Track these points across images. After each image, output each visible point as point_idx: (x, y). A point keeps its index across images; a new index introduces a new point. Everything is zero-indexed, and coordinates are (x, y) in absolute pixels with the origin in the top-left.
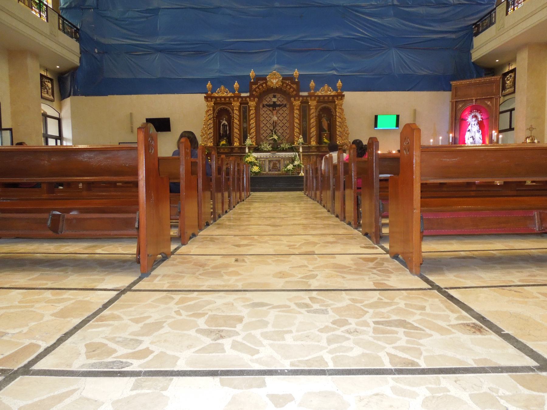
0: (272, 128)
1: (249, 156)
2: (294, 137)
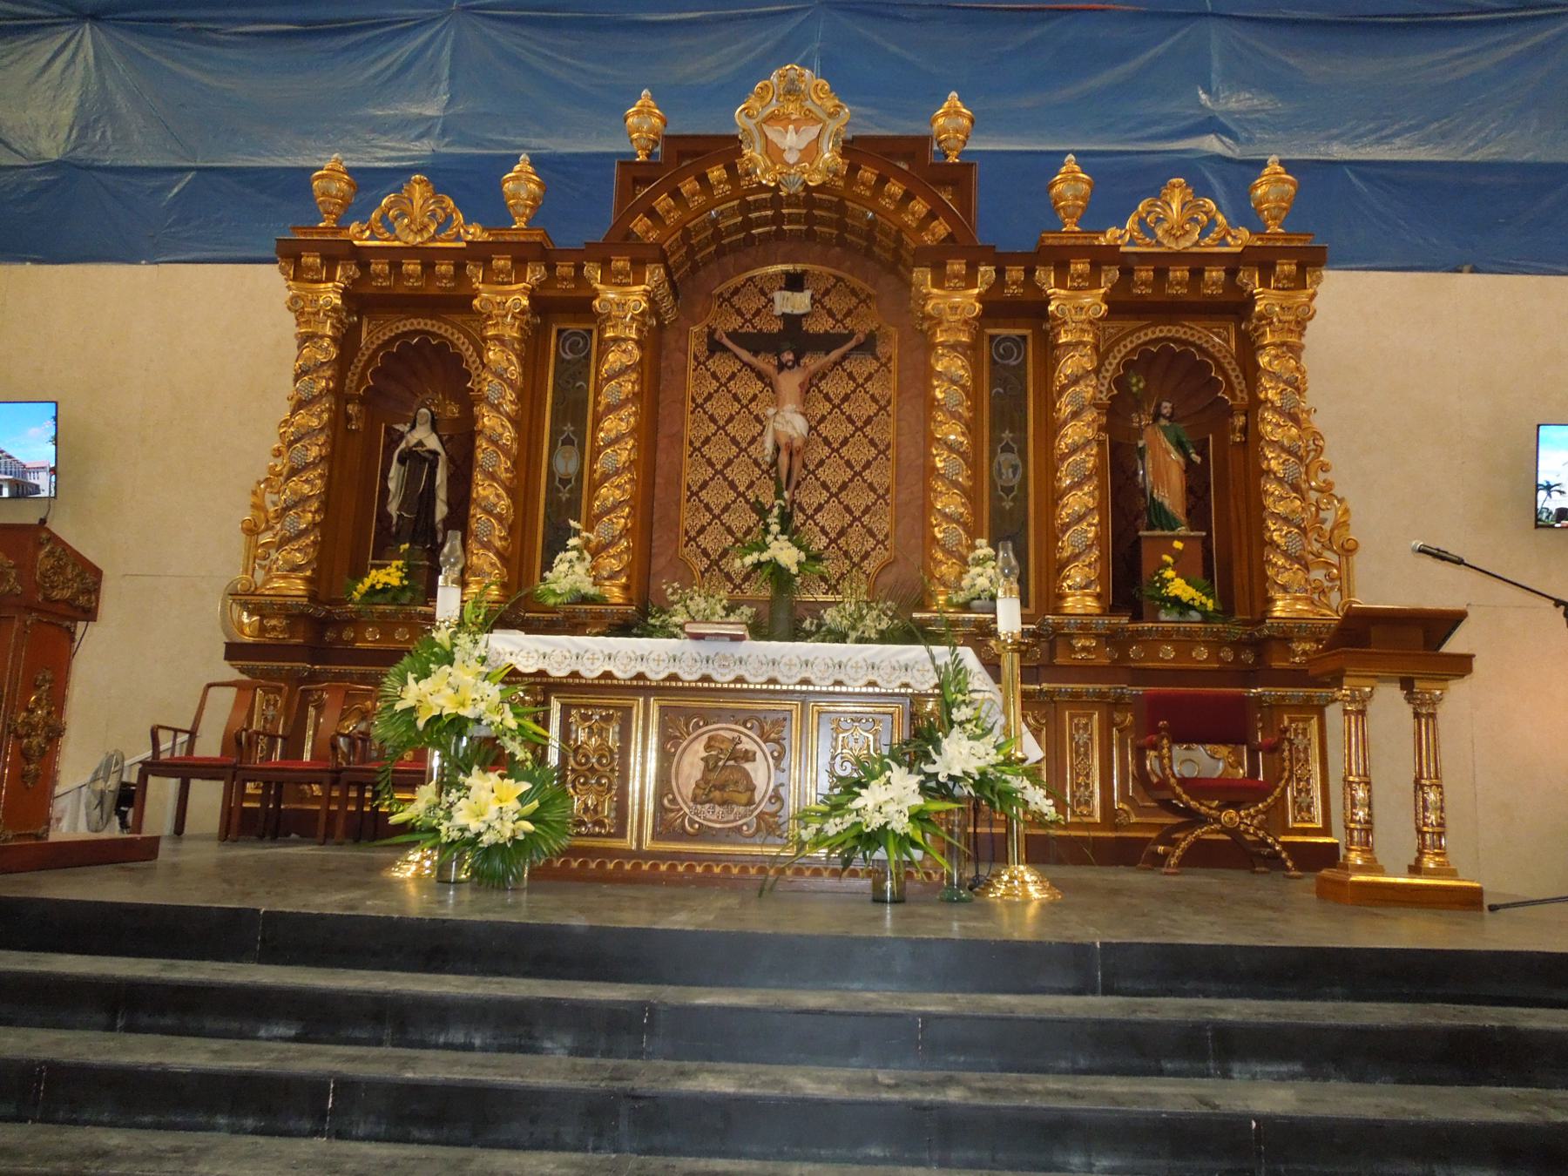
1: (448, 659)
2: (928, 563)
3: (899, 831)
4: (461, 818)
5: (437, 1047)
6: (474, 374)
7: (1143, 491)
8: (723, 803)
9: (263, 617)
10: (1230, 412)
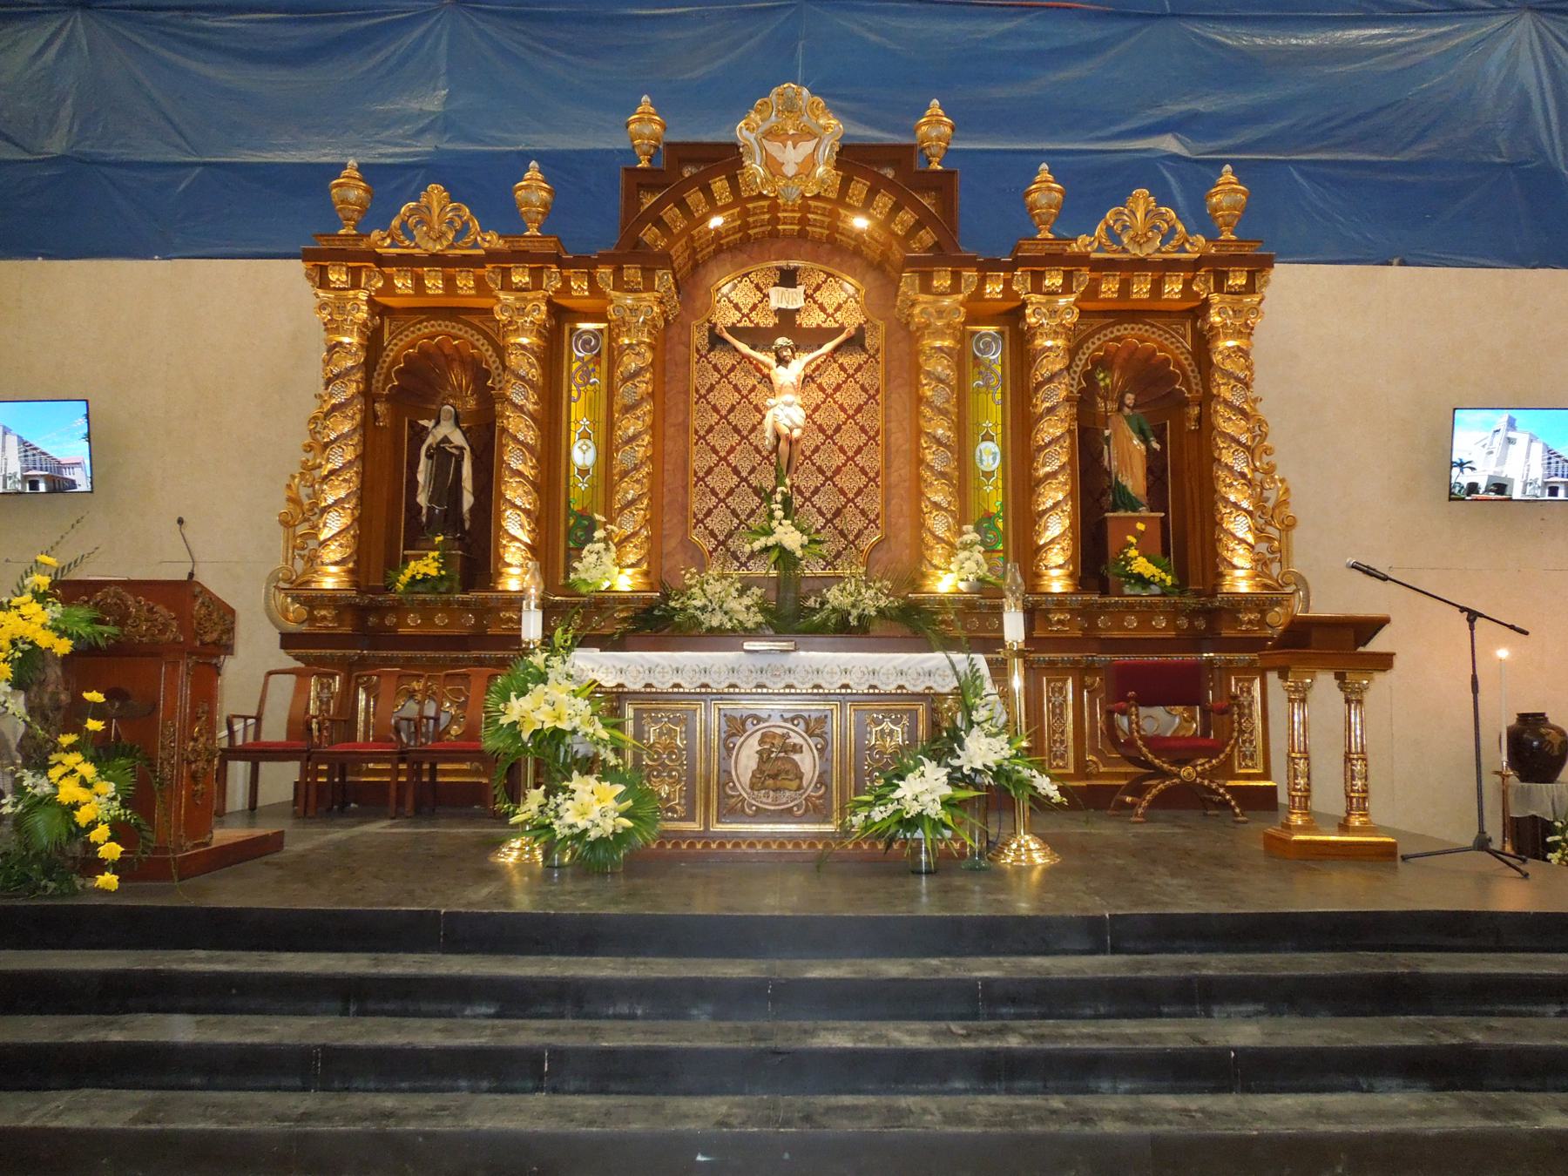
0: (769, 484)
1: (542, 678)
3: (933, 816)
4: (569, 818)
5: (608, 1017)
6: (494, 373)
7: (1109, 474)
8: (776, 790)
9: (312, 608)
10: (1185, 403)
